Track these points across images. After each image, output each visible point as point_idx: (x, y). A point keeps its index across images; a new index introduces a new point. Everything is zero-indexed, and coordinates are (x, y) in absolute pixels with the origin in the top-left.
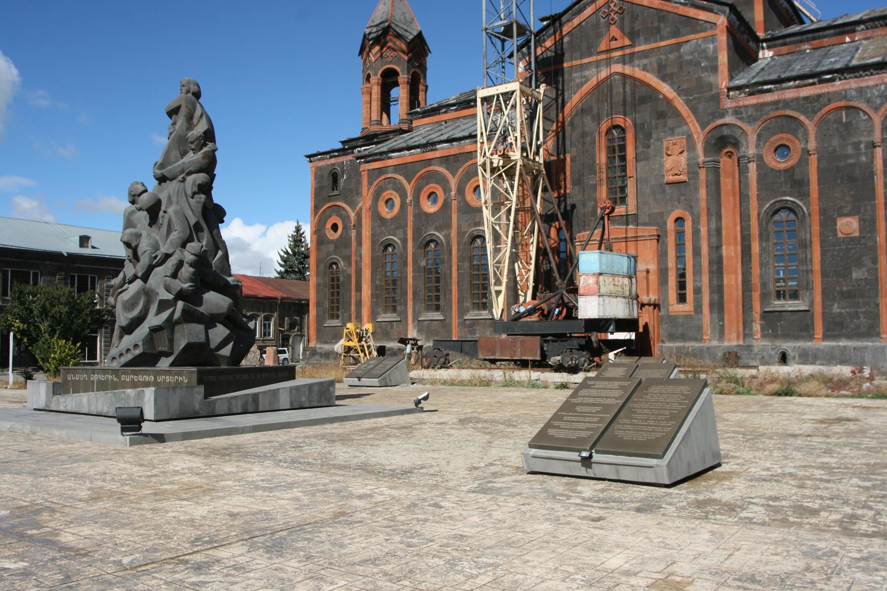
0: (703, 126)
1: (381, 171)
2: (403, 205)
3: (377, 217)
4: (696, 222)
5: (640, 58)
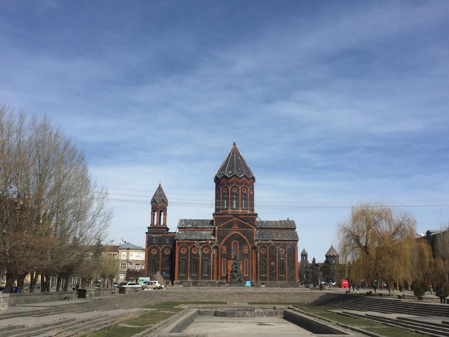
1: (182, 243)
2: (188, 251)
3: (180, 253)
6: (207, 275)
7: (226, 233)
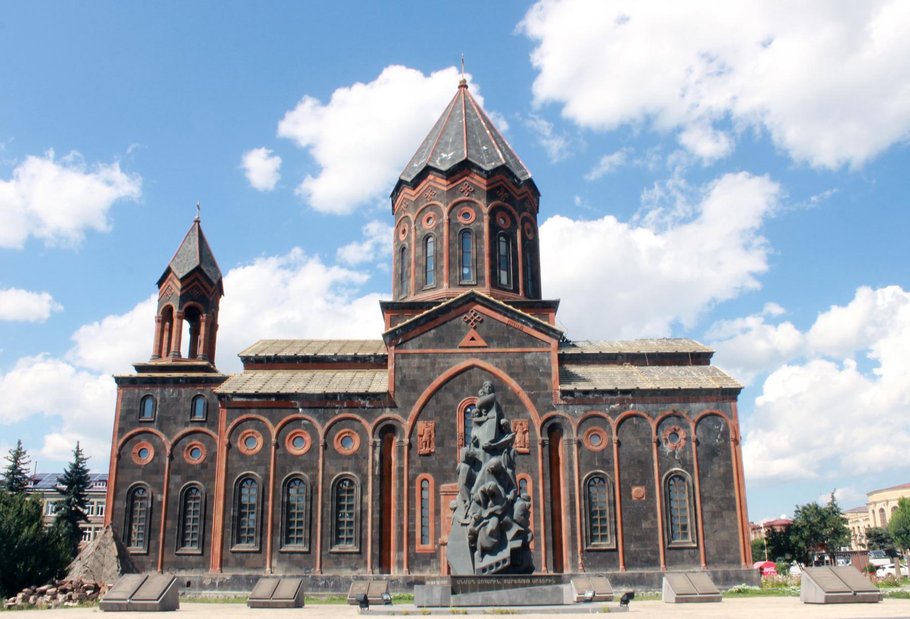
0: (541, 414)
2: (266, 445)
4: (535, 484)
5: (494, 357)
6: (351, 547)
7: (433, 364)
